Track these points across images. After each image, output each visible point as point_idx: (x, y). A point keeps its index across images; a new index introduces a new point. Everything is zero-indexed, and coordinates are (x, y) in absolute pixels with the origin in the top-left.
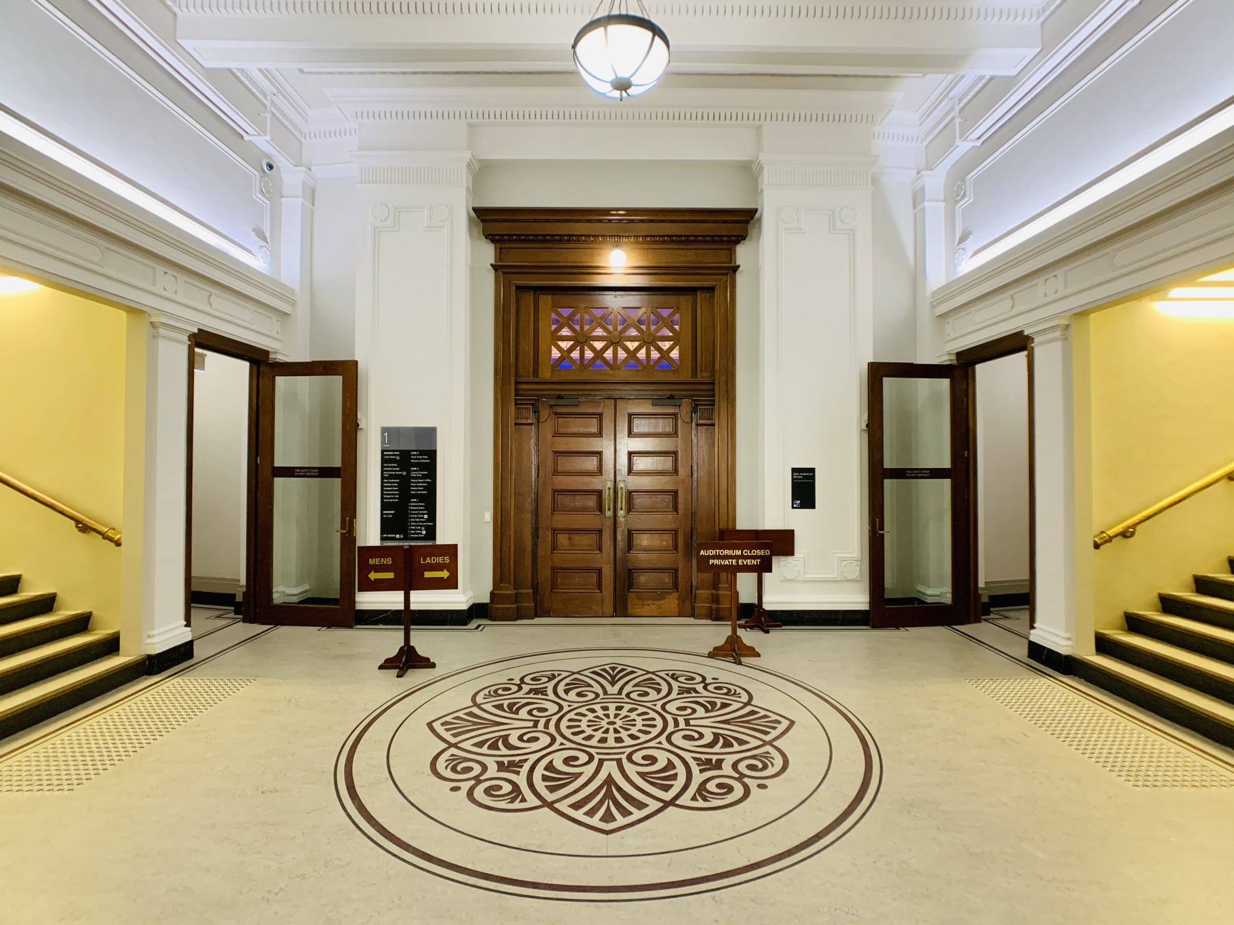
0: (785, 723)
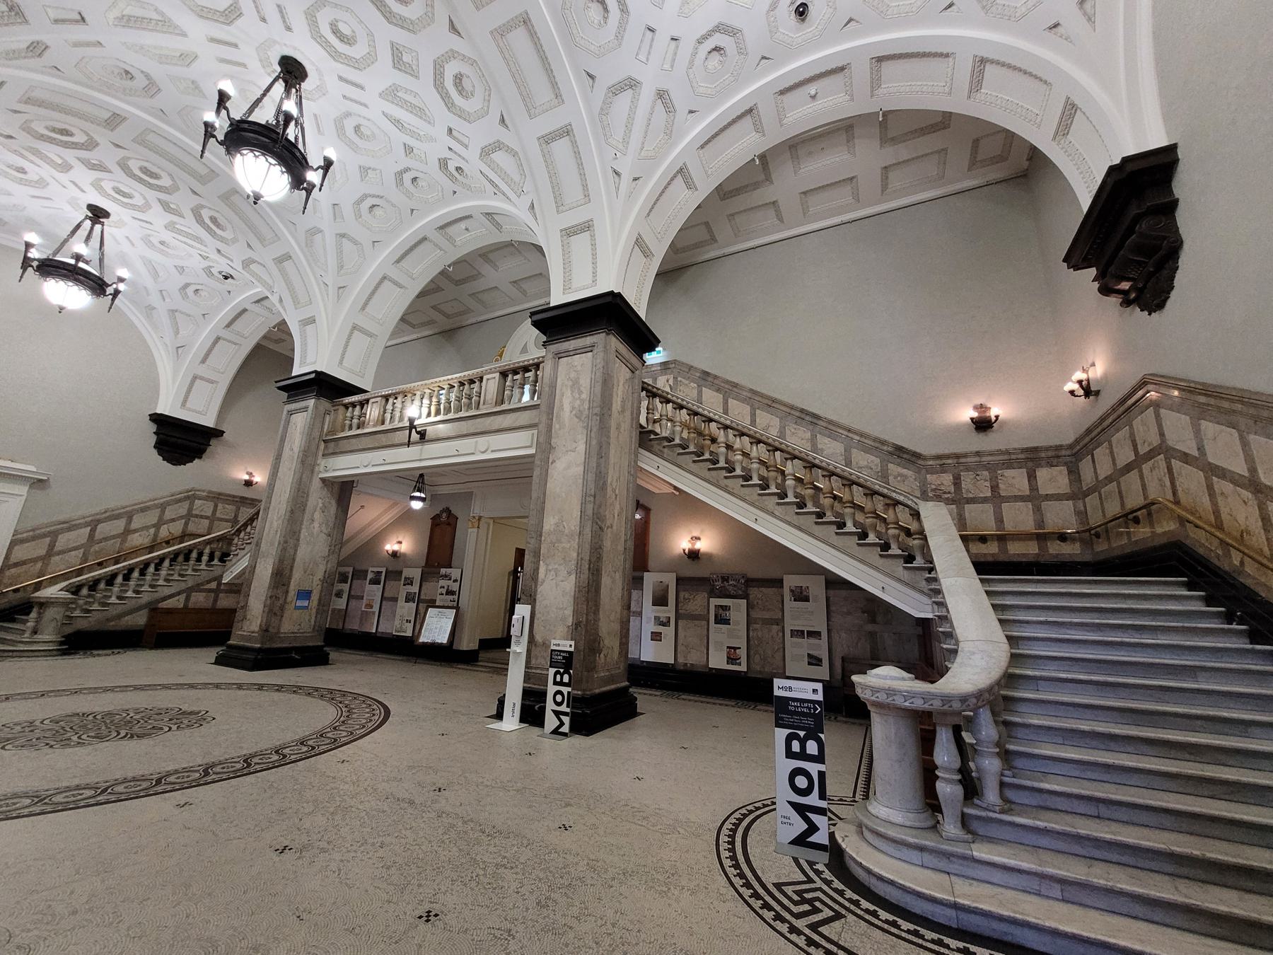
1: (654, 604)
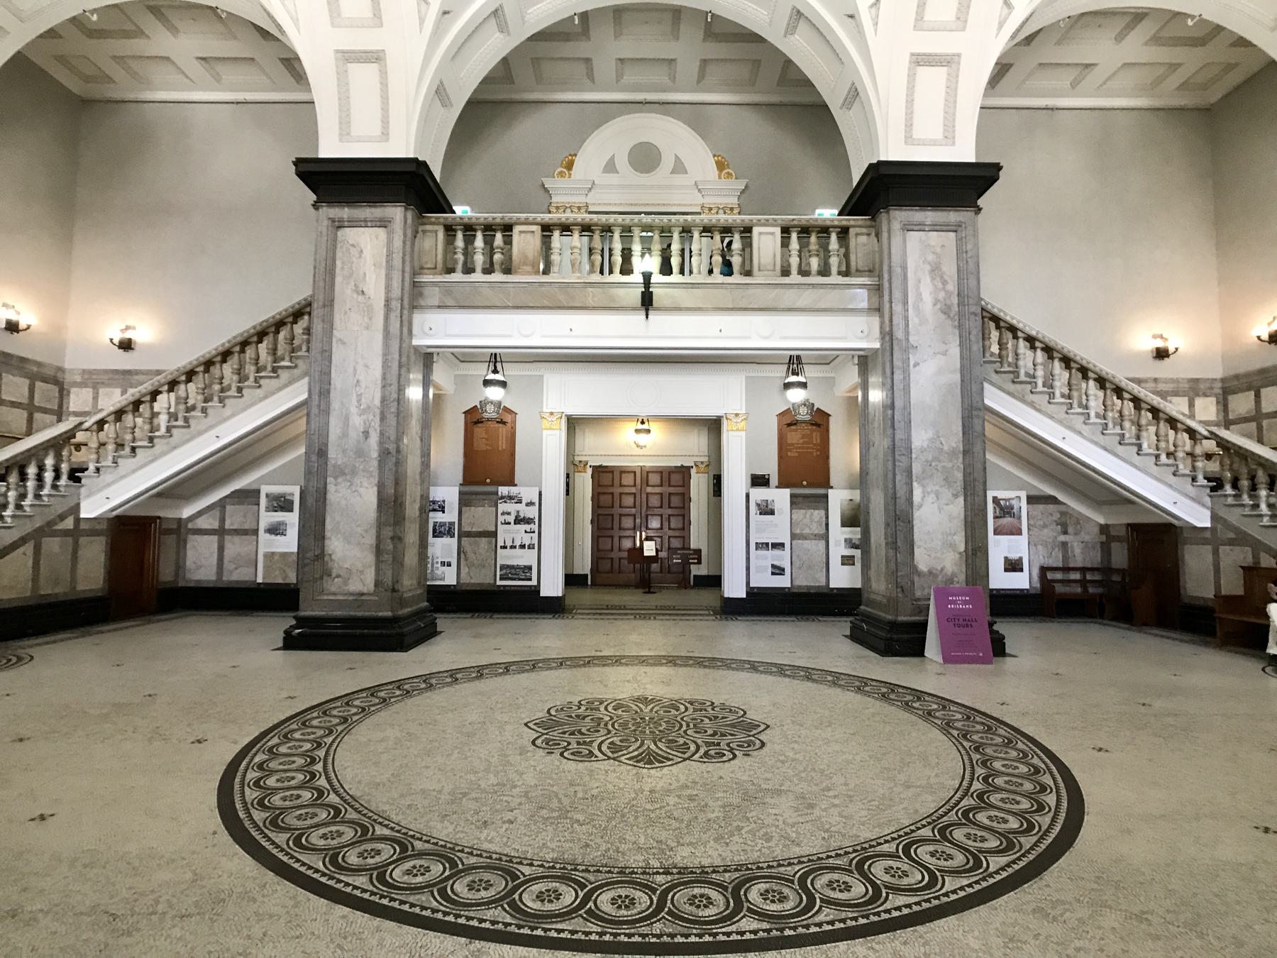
0: (763, 727)
1: (843, 525)
